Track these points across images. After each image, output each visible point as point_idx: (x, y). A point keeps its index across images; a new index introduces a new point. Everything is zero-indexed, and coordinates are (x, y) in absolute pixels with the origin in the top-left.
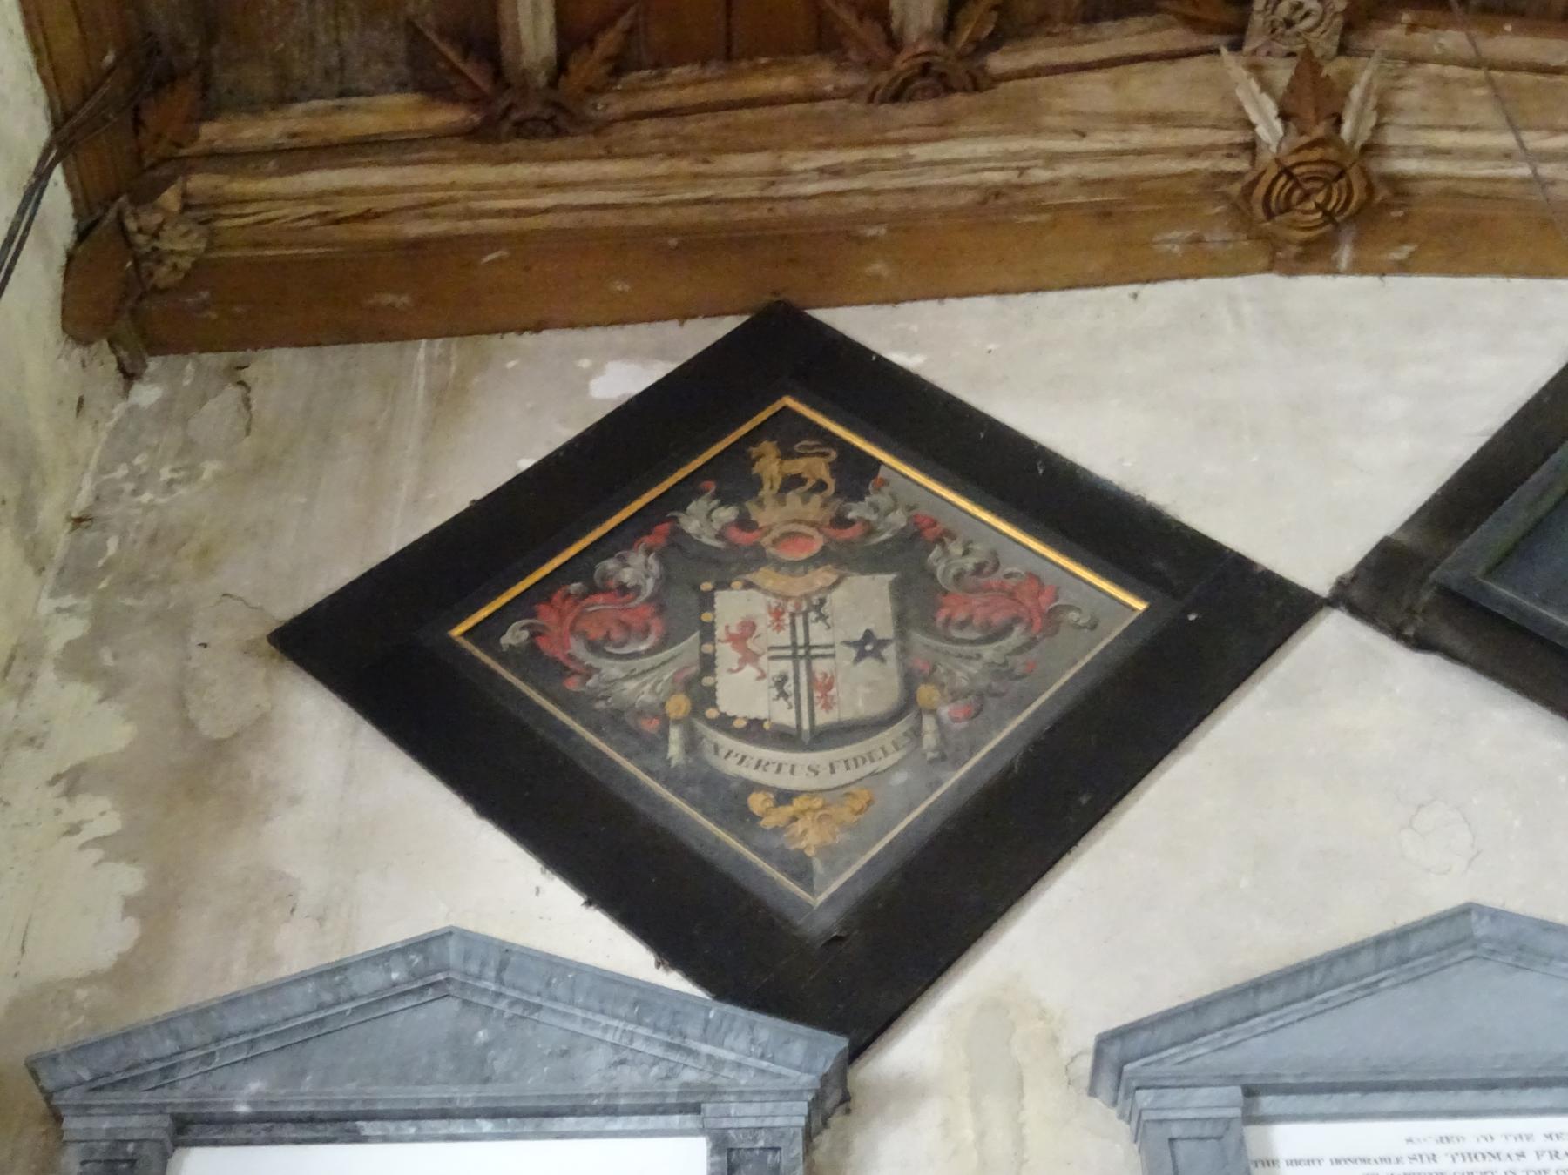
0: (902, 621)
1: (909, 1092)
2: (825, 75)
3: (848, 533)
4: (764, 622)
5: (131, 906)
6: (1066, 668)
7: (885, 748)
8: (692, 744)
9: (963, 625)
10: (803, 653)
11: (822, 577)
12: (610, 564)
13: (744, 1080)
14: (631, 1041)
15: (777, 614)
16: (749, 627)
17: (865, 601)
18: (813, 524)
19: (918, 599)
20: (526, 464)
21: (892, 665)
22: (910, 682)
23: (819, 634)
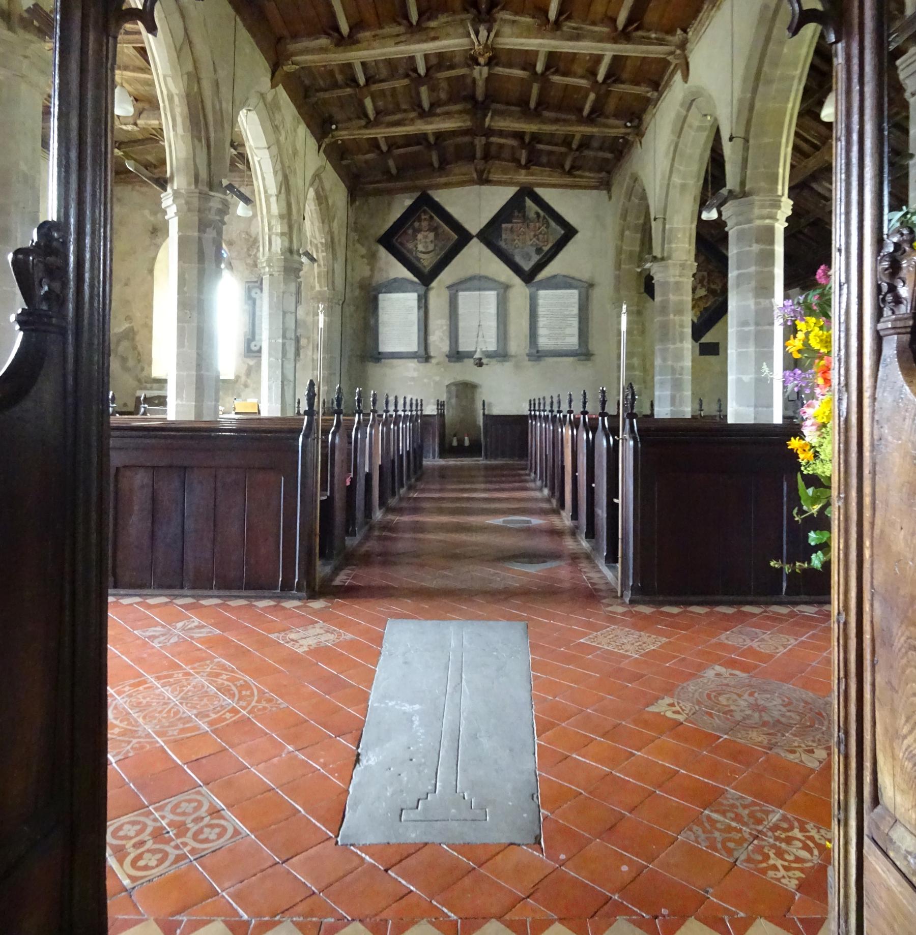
1: (433, 288)
6: (450, 244)
10: (426, 242)
17: (431, 235)
19: (436, 236)
22: (435, 246)
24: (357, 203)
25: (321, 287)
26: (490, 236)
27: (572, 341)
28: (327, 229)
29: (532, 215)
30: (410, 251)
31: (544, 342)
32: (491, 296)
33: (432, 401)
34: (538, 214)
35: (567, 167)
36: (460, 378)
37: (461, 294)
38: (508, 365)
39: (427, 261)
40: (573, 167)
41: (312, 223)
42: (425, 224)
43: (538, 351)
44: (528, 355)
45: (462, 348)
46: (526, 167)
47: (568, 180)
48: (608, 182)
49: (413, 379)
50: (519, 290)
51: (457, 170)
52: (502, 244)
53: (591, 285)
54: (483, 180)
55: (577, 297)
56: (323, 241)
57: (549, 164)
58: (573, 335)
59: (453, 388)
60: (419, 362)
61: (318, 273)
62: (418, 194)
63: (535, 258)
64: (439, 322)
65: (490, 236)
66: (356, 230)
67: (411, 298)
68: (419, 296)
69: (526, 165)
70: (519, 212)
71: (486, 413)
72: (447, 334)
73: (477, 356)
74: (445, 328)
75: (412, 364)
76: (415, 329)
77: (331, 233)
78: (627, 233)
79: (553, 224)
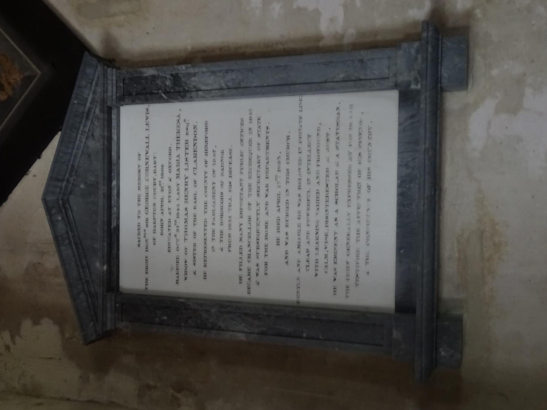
5: (36, 322)
13: (99, 90)
14: (85, 132)
60: (463, 81)
75: (477, 123)
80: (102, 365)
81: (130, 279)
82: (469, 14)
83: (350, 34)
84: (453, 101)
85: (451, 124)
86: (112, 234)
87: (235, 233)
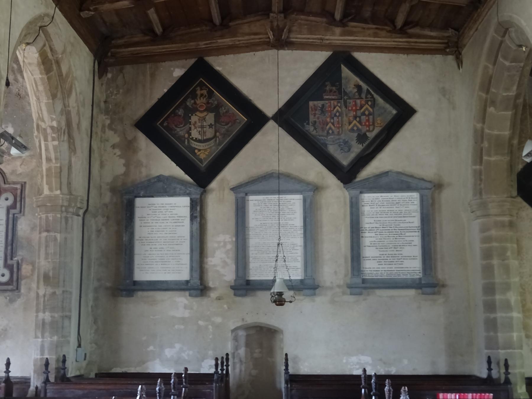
0: (215, 121)
1: (212, 190)
2: (204, 28)
3: (209, 105)
4: (197, 121)
5: (124, 165)
7: (212, 143)
8: (188, 142)
9: (223, 122)
10: (202, 127)
11: (205, 113)
12: (177, 111)
15: (199, 120)
16: (196, 122)
17: (210, 118)
18: (204, 103)
20: (166, 90)
21: (214, 129)
22: (216, 132)
23: (205, 124)
24: (109, 75)
25: (51, 189)
26: (293, 118)
27: (412, 265)
28: (59, 106)
29: (350, 88)
30: (181, 139)
31: (372, 267)
32: (295, 202)
33: (210, 353)
34: (359, 87)
35: (400, 21)
36: (250, 320)
37: (254, 202)
38: (321, 301)
39: (204, 153)
40: (406, 23)
41: (38, 99)
42: (201, 101)
43: (364, 281)
44: (350, 287)
45: (255, 275)
46: (342, 23)
47: (401, 41)
48: (457, 43)
49: (183, 320)
50: (334, 194)
51: (246, 29)
52: (310, 129)
53: (439, 186)
54: (281, 43)
55: (417, 202)
56: (55, 124)
57: (374, 19)
58: (414, 258)
59: (242, 334)
60: (190, 295)
61: (49, 170)
62: (191, 62)
63: (357, 149)
64: (221, 238)
65: (293, 118)
66: (107, 112)
67: (181, 205)
68: (192, 201)
69: (341, 21)
70: (333, 85)
71: (291, 371)
72: (232, 255)
73: (276, 289)
74: (229, 247)
75: (182, 300)
76: (186, 248)
77: (66, 113)
78: (491, 110)
79: (380, 100)
80: (113, 190)
81: (139, 202)
82: (209, 297)
83: (206, 266)
84: (187, 293)
85: (182, 293)
86: (153, 197)
87: (153, 235)
